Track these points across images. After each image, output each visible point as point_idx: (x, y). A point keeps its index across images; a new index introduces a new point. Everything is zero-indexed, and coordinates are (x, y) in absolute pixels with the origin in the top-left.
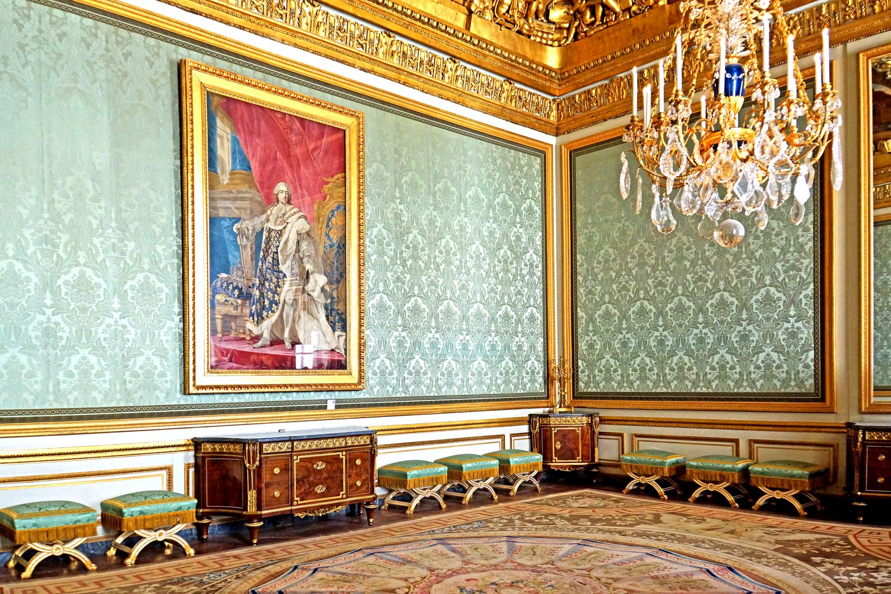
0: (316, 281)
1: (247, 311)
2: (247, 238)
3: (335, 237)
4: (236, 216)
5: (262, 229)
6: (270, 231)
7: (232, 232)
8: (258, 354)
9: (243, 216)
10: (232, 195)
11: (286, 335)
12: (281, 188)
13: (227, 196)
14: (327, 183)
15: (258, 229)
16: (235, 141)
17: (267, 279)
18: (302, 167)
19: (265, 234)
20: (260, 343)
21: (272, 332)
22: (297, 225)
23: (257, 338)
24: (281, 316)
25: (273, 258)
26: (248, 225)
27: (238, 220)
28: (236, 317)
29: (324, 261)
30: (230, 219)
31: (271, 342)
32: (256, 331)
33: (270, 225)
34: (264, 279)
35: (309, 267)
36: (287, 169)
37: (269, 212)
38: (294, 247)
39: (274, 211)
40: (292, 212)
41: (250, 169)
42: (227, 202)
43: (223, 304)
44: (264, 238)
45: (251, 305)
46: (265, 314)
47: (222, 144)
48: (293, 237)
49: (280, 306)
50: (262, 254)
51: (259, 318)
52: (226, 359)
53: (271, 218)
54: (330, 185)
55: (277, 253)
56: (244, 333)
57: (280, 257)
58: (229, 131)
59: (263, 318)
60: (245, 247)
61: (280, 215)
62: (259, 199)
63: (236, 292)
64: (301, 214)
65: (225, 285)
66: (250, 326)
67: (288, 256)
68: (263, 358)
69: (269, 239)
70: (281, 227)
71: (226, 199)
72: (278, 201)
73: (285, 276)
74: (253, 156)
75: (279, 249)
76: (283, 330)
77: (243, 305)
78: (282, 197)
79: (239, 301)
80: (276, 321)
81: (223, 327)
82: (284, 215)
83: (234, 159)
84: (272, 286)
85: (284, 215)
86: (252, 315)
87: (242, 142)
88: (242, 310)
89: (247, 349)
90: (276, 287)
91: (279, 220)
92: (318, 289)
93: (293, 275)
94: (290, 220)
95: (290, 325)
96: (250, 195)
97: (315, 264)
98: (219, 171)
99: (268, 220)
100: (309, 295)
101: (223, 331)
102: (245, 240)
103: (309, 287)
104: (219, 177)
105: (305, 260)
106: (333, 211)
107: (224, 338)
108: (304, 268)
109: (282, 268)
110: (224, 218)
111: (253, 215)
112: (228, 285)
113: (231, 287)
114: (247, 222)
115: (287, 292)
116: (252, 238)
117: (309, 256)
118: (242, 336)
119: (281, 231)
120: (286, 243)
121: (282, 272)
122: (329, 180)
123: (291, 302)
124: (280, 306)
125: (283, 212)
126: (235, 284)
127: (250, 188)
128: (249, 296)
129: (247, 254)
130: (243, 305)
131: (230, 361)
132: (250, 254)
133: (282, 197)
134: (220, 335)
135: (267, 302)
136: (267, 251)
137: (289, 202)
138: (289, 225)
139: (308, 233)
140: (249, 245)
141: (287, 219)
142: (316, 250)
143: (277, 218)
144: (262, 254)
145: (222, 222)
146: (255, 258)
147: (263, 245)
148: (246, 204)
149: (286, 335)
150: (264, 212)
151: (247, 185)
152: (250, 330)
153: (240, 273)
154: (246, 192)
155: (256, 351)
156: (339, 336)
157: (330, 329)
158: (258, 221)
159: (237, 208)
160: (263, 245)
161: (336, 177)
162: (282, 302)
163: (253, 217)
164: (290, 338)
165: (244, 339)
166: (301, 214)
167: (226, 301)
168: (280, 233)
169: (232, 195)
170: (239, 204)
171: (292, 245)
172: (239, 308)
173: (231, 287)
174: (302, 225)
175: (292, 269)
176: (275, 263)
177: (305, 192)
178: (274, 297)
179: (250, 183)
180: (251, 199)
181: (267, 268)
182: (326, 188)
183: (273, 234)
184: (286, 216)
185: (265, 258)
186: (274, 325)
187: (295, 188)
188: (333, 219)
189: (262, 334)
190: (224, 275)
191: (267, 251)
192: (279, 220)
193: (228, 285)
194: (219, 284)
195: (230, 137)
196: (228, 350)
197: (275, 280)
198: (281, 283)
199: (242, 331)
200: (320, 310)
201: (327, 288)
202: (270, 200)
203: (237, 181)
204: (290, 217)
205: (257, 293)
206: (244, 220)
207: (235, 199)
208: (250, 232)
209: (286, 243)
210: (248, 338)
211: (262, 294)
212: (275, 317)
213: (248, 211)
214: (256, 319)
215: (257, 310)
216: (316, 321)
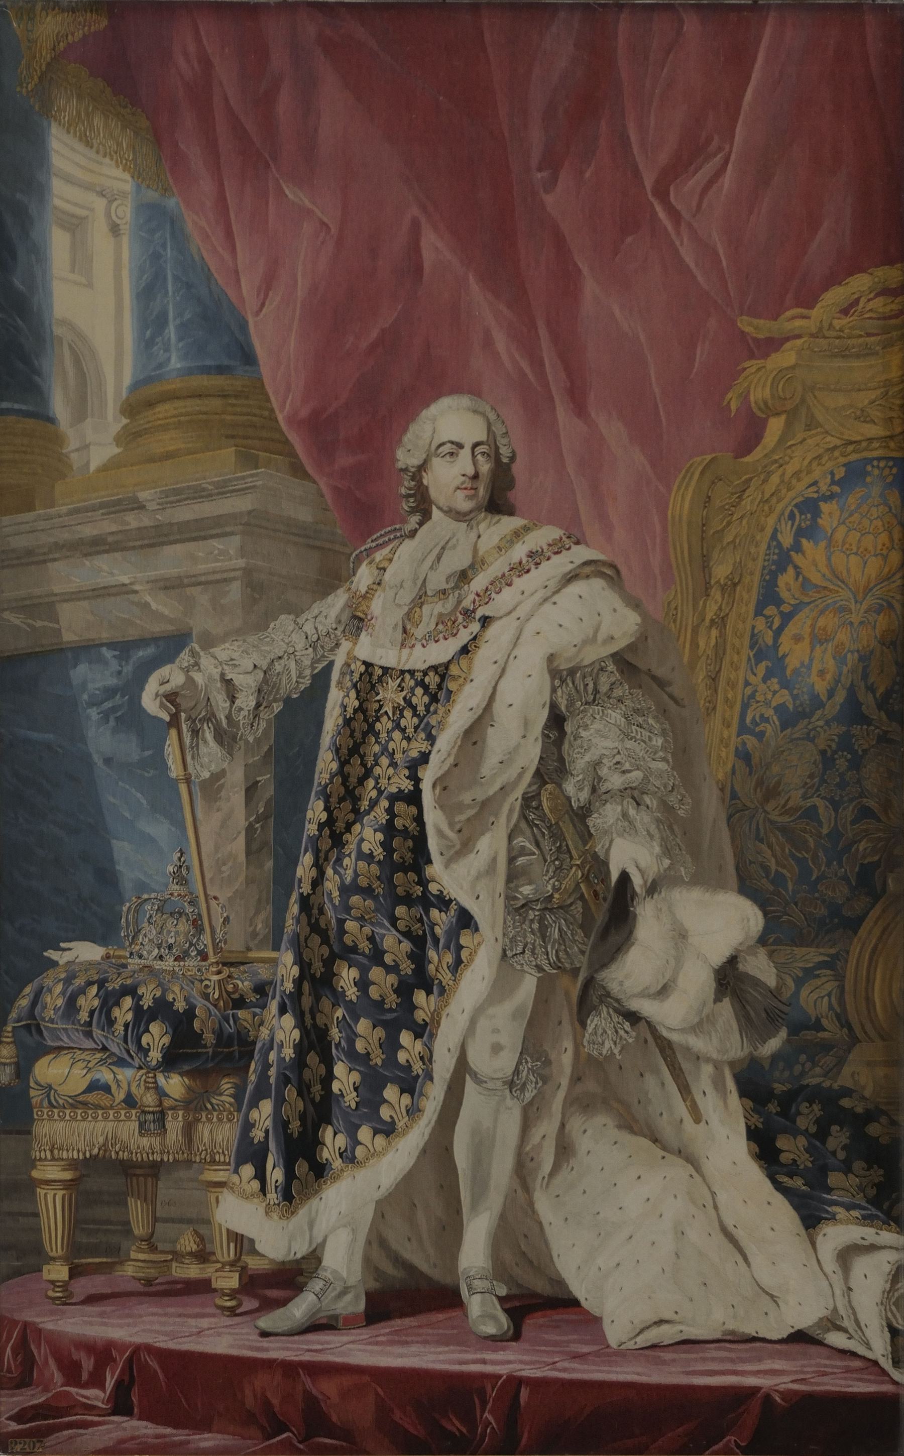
0: (681, 935)
1: (218, 1133)
2: (226, 738)
3: (825, 658)
4: (158, 628)
5: (321, 681)
6: (370, 678)
7: (131, 718)
8: (289, 1369)
9: (200, 622)
10: (133, 521)
11: (474, 1253)
12: (447, 432)
13: (107, 526)
14: (772, 345)
15: (294, 678)
16: (153, 218)
17: (349, 953)
18: (590, 287)
19: (338, 701)
20: (300, 1309)
21: (377, 1240)
22: (548, 616)
23: (290, 1278)
24: (439, 1148)
25: (389, 829)
26: (235, 666)
27: (171, 645)
28: (155, 1169)
29: (736, 810)
30: (124, 648)
31: (370, 1297)
32: (275, 1239)
33: (377, 648)
34: (323, 952)
35: (630, 853)
36: (485, 309)
37: (364, 576)
38: (531, 754)
39: (401, 565)
40: (519, 552)
41: (249, 358)
42: (103, 562)
43: (77, 1103)
44: (332, 721)
45: (244, 1101)
46: (332, 1142)
47: (81, 260)
48: (522, 695)
49: (434, 1097)
50: (316, 811)
51: (299, 1162)
52: (96, 1396)
53: (376, 606)
54: (786, 358)
55: (414, 798)
56: (203, 1256)
57: (432, 816)
58: (119, 179)
59: (320, 1170)
60: (212, 787)
61: (437, 581)
62: (304, 515)
63: (157, 1036)
64: (581, 553)
65: (89, 1001)
66: (242, 1211)
67: (486, 806)
68: (329, 1388)
69: (361, 725)
70: (441, 652)
71: (97, 546)
72: (423, 505)
73: (465, 920)
74: (268, 284)
75: (428, 775)
76: (450, 1231)
77: (195, 1105)
78: (447, 479)
79: (175, 1085)
80: (408, 1180)
81: (77, 1222)
82: (464, 577)
83: (151, 325)
84: (383, 983)
85: (464, 577)
86: (252, 1154)
87: (193, 223)
88: (189, 1130)
89: (218, 1336)
90: (404, 990)
91: (431, 611)
92: (696, 980)
93: (517, 909)
94: (505, 598)
95: (495, 1201)
96: (241, 504)
97: (679, 832)
98: (60, 406)
99: (357, 622)
100: (633, 1017)
101: (74, 1250)
102: (210, 747)
103: (634, 972)
104: (58, 440)
105: (607, 816)
106: (810, 507)
107: (85, 1286)
108: (601, 865)
109: (449, 877)
110: (87, 650)
111: (264, 600)
112: (110, 1001)
113: (123, 1013)
114: (222, 652)
115: (479, 1009)
116: (256, 733)
117: (634, 795)
118: (193, 1271)
119: (442, 670)
120: (474, 735)
121: (444, 902)
122: (791, 321)
123: (506, 1063)
124: (434, 1097)
125: (457, 560)
126: (148, 995)
127: (248, 460)
128: (236, 1051)
129: (221, 832)
130: (195, 1105)
131: (120, 1405)
132: (240, 819)
133: (447, 479)
134: (59, 1272)
135: (345, 1079)
136: (347, 796)
137: (497, 503)
138: (498, 636)
139: (626, 663)
140: (237, 777)
141: (485, 596)
142: (682, 755)
143: (420, 600)
144: (316, 811)
145: (81, 672)
146: (275, 832)
147: (326, 763)
148: (224, 554)
149: (474, 1253)
150: (332, 577)
151: (229, 453)
152: (238, 1239)
153: (177, 931)
154: (223, 490)
155: (276, 1351)
156: (847, 1255)
157: (784, 1214)
158: (290, 643)
159: (169, 585)
160: (326, 763)
161: (835, 296)
162: (444, 1065)
163: (268, 618)
164: (500, 1271)
165: (202, 1287)
166: (581, 553)
167: (94, 1086)
168: (438, 685)
169: (133, 521)
170: (173, 560)
171: (514, 747)
172: (175, 1125)
173: (123, 1013)
174: (579, 617)
175: (513, 876)
176: (402, 848)
177: (613, 430)
178: (391, 1045)
179: (255, 438)
180: (254, 525)
181: (346, 890)
182: (757, 383)
183: (390, 694)
184: (479, 582)
185: (335, 833)
186: (398, 1201)
187: (535, 407)
188: (812, 557)
189: (314, 1258)
190: (87, 952)
191: (351, 795)
192: (431, 611)
193: (110, 1001)
194: (54, 1000)
195: (125, 213)
196: (104, 1353)
197: (396, 948)
198: (438, 961)
199: (187, 1243)
200: (709, 1103)
201: (761, 968)
202: (371, 501)
203: (169, 441)
204: (503, 581)
205: (284, 1031)
206: (209, 642)
207: (158, 537)
208: (246, 701)
209: (474, 735)
210: (231, 1281)
211: (315, 1040)
212: (393, 1162)
213: (235, 591)
214: (276, 1175)
215: (281, 1124)
216: (679, 1170)
